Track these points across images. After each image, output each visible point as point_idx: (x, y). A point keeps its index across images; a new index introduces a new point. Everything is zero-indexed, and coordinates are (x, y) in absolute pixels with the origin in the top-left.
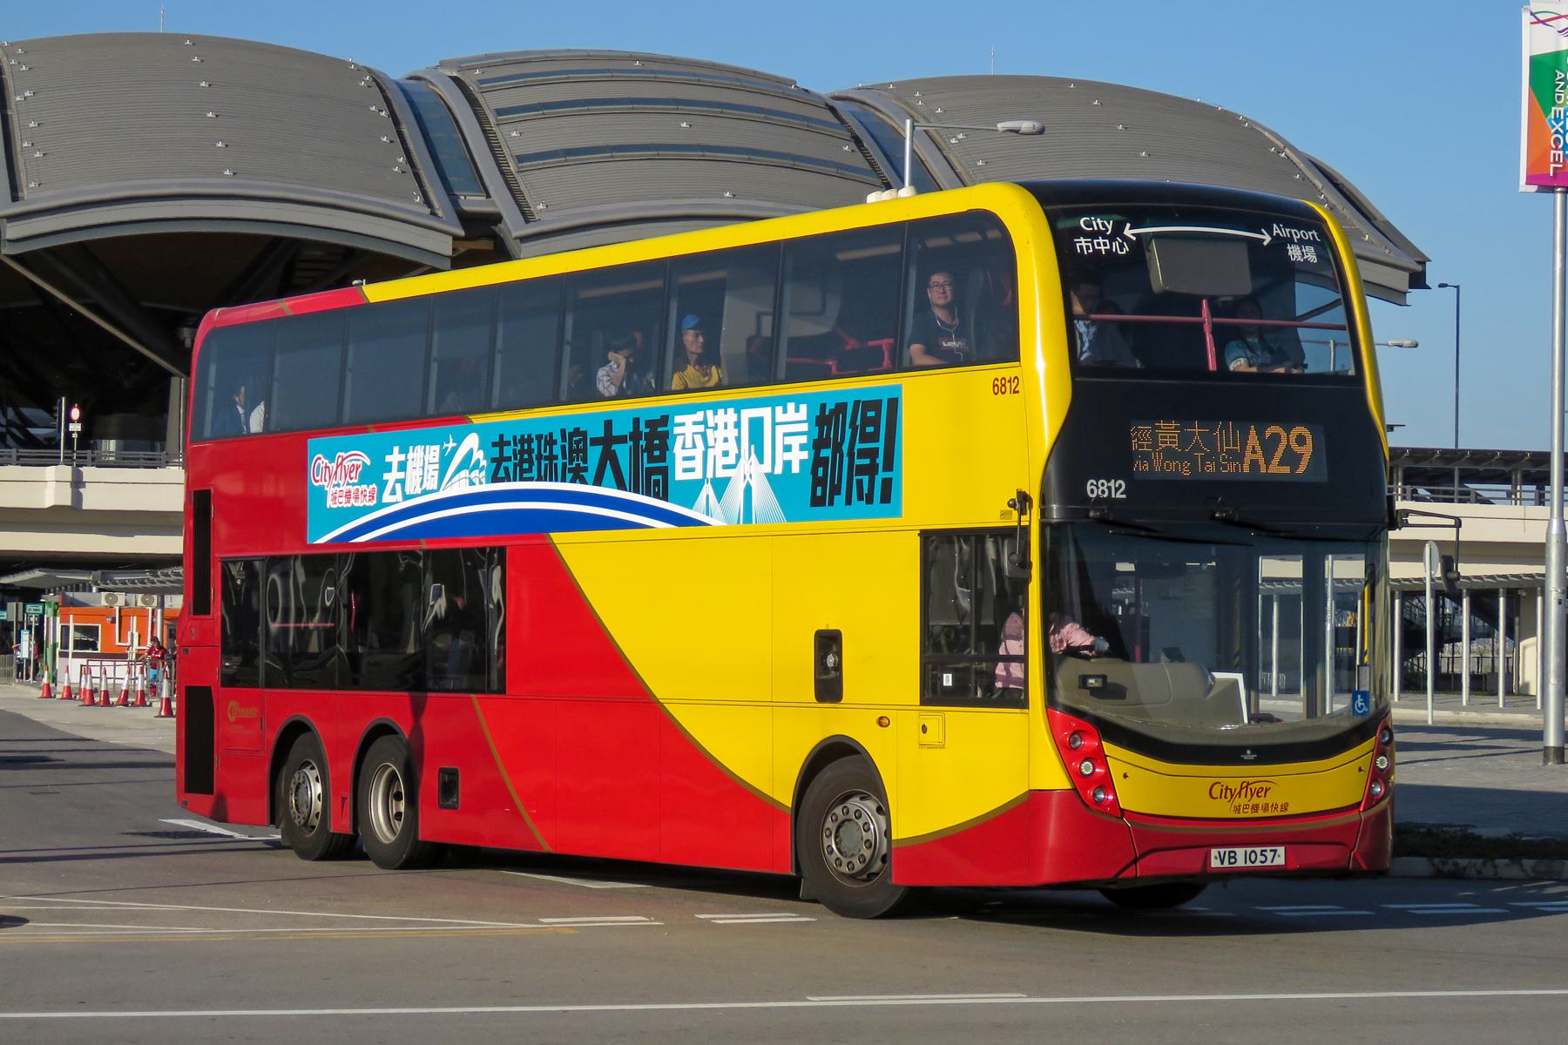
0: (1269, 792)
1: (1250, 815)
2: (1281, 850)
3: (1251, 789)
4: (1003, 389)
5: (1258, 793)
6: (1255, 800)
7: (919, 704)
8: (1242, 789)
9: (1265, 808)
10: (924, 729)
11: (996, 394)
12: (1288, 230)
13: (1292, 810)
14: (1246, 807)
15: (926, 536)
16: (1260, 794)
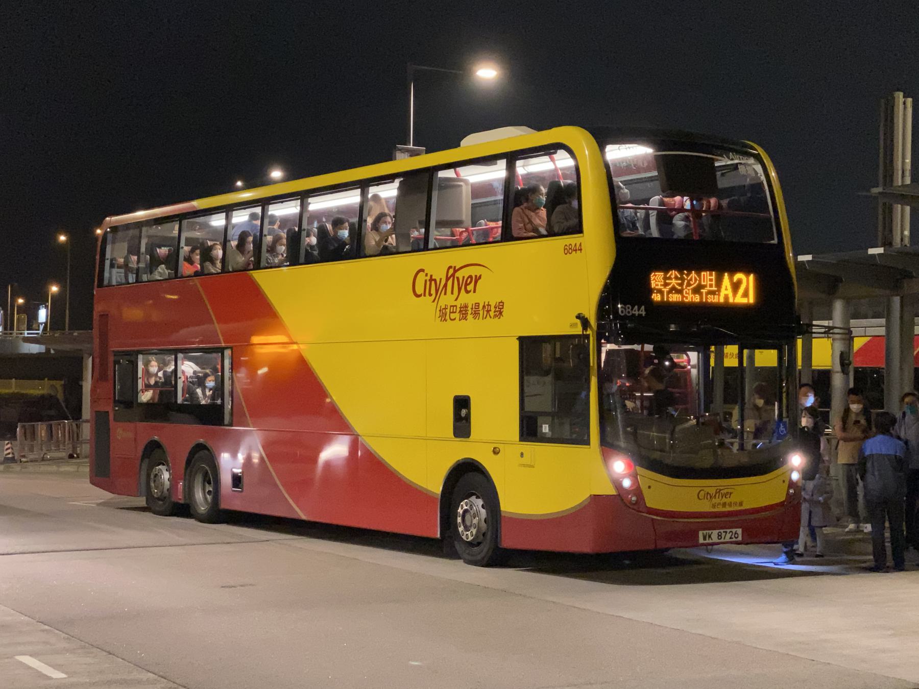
0: (732, 495)
1: (720, 509)
2: (739, 531)
3: (722, 493)
4: (570, 252)
5: (726, 495)
6: (724, 500)
7: (518, 440)
8: (716, 493)
9: (730, 504)
10: (522, 455)
11: (566, 254)
12: (738, 156)
13: (746, 506)
14: (719, 504)
15: (522, 340)
16: (727, 496)
